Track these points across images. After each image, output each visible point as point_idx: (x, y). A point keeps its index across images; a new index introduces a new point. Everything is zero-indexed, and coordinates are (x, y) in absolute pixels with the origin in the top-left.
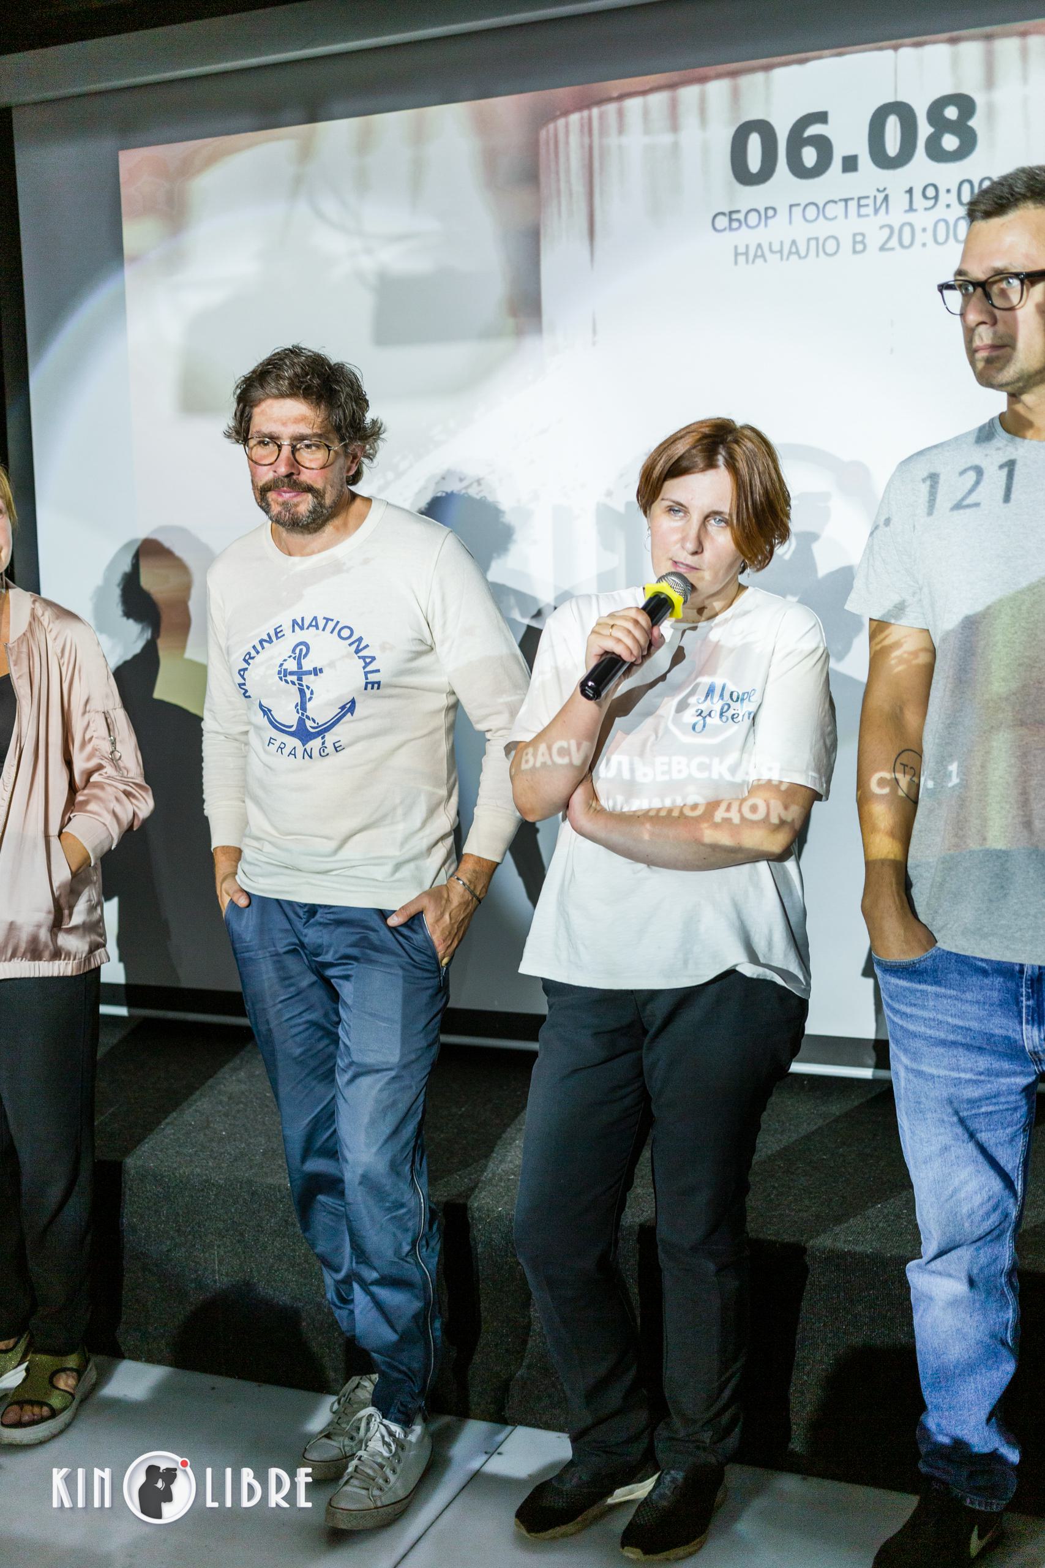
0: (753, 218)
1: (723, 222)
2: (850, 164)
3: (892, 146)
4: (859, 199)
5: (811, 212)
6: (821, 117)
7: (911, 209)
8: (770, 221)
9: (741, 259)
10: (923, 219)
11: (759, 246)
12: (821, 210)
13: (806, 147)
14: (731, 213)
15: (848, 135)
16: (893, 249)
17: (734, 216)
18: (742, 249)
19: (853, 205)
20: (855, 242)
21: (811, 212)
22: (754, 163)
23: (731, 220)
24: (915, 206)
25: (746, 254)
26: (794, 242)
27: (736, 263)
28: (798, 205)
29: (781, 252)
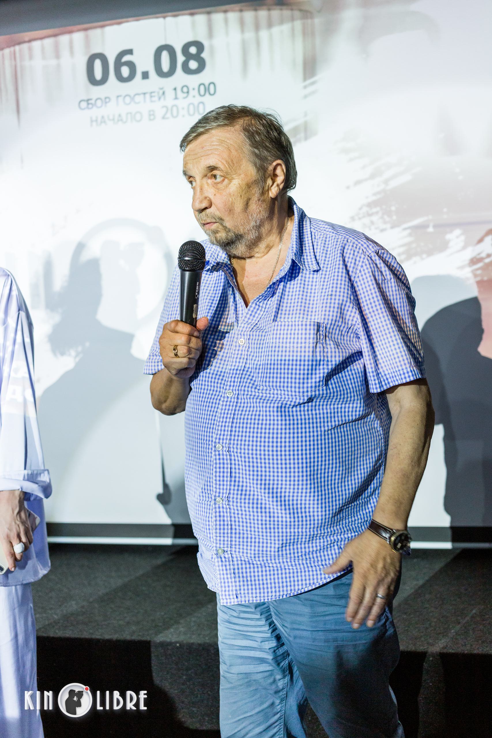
0: (99, 103)
1: (84, 105)
2: (145, 75)
3: (165, 66)
4: (151, 93)
5: (128, 99)
6: (130, 52)
7: (176, 98)
8: (108, 104)
9: (94, 124)
10: (182, 103)
11: (103, 117)
12: (132, 99)
13: (123, 67)
14: (88, 100)
15: (144, 61)
16: (168, 118)
17: (90, 102)
18: (94, 119)
19: (148, 96)
20: (150, 115)
21: (128, 99)
22: (98, 74)
23: (88, 104)
25: (96, 121)
26: (120, 115)
27: (91, 125)
28: (121, 96)
29: (113, 120)
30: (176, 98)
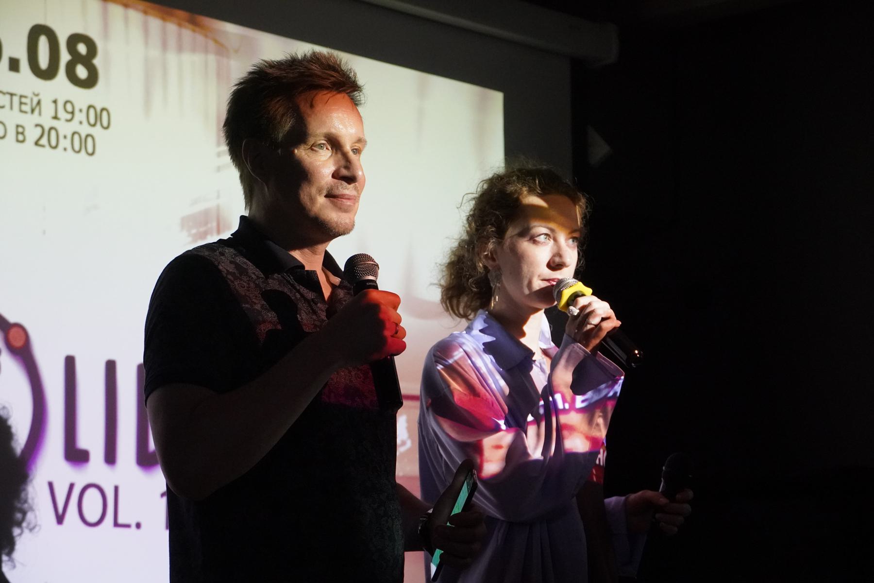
24: (59, 115)
30: (56, 118)
